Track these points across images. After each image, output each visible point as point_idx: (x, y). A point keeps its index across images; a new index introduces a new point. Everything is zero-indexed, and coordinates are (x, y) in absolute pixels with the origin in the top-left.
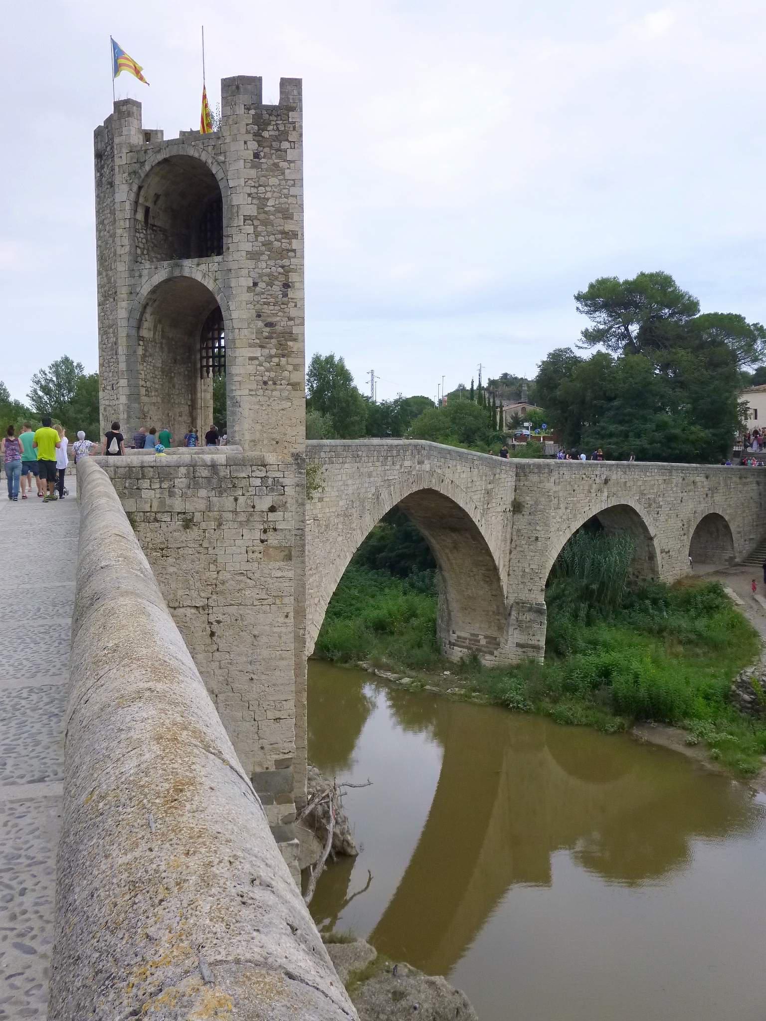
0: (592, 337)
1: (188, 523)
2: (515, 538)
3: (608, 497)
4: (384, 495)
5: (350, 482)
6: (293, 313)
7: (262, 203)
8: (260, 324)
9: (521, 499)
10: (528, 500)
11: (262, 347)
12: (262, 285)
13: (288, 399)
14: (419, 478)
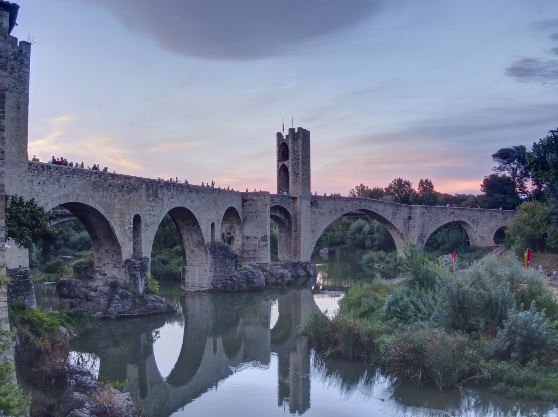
0: (500, 169)
1: (253, 201)
2: (410, 227)
3: (453, 218)
4: (345, 209)
5: (332, 205)
6: (299, 170)
7: (294, 150)
8: (294, 172)
9: (411, 216)
10: (413, 216)
11: (294, 176)
12: (294, 165)
13: (298, 186)
14: (360, 206)
